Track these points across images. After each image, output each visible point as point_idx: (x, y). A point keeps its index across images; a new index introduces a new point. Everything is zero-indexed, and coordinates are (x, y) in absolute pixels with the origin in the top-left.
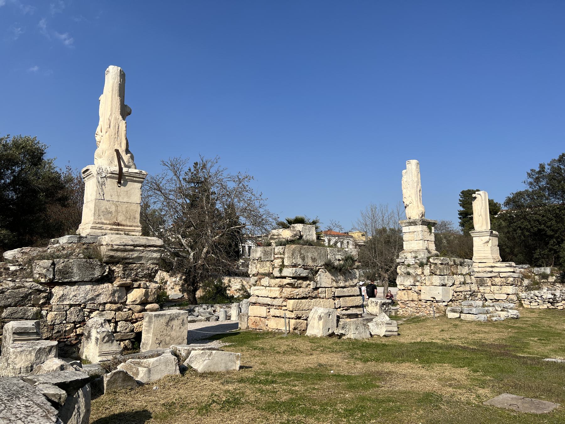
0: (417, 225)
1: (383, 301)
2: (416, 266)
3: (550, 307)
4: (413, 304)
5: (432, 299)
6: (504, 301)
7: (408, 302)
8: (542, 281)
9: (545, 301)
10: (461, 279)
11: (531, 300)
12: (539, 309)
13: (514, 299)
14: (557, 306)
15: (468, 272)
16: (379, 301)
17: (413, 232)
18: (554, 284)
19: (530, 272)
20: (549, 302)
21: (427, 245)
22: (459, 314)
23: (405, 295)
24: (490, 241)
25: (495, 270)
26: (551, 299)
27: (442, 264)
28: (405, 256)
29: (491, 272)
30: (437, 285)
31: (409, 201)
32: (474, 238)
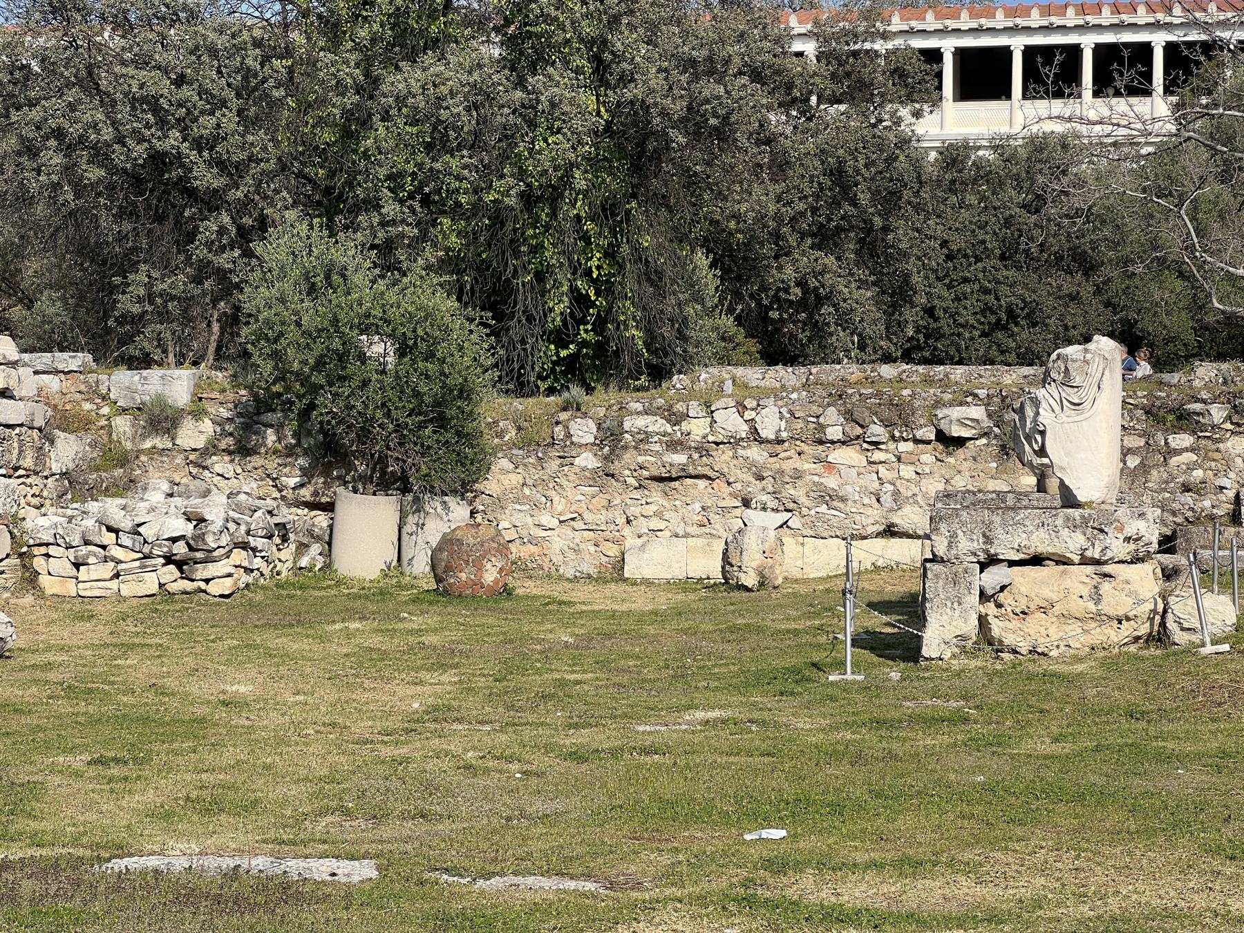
3: (173, 587)
8: (148, 444)
11: (84, 550)
14: (207, 581)
18: (200, 459)
19: (94, 393)
20: (169, 559)
26: (182, 543)
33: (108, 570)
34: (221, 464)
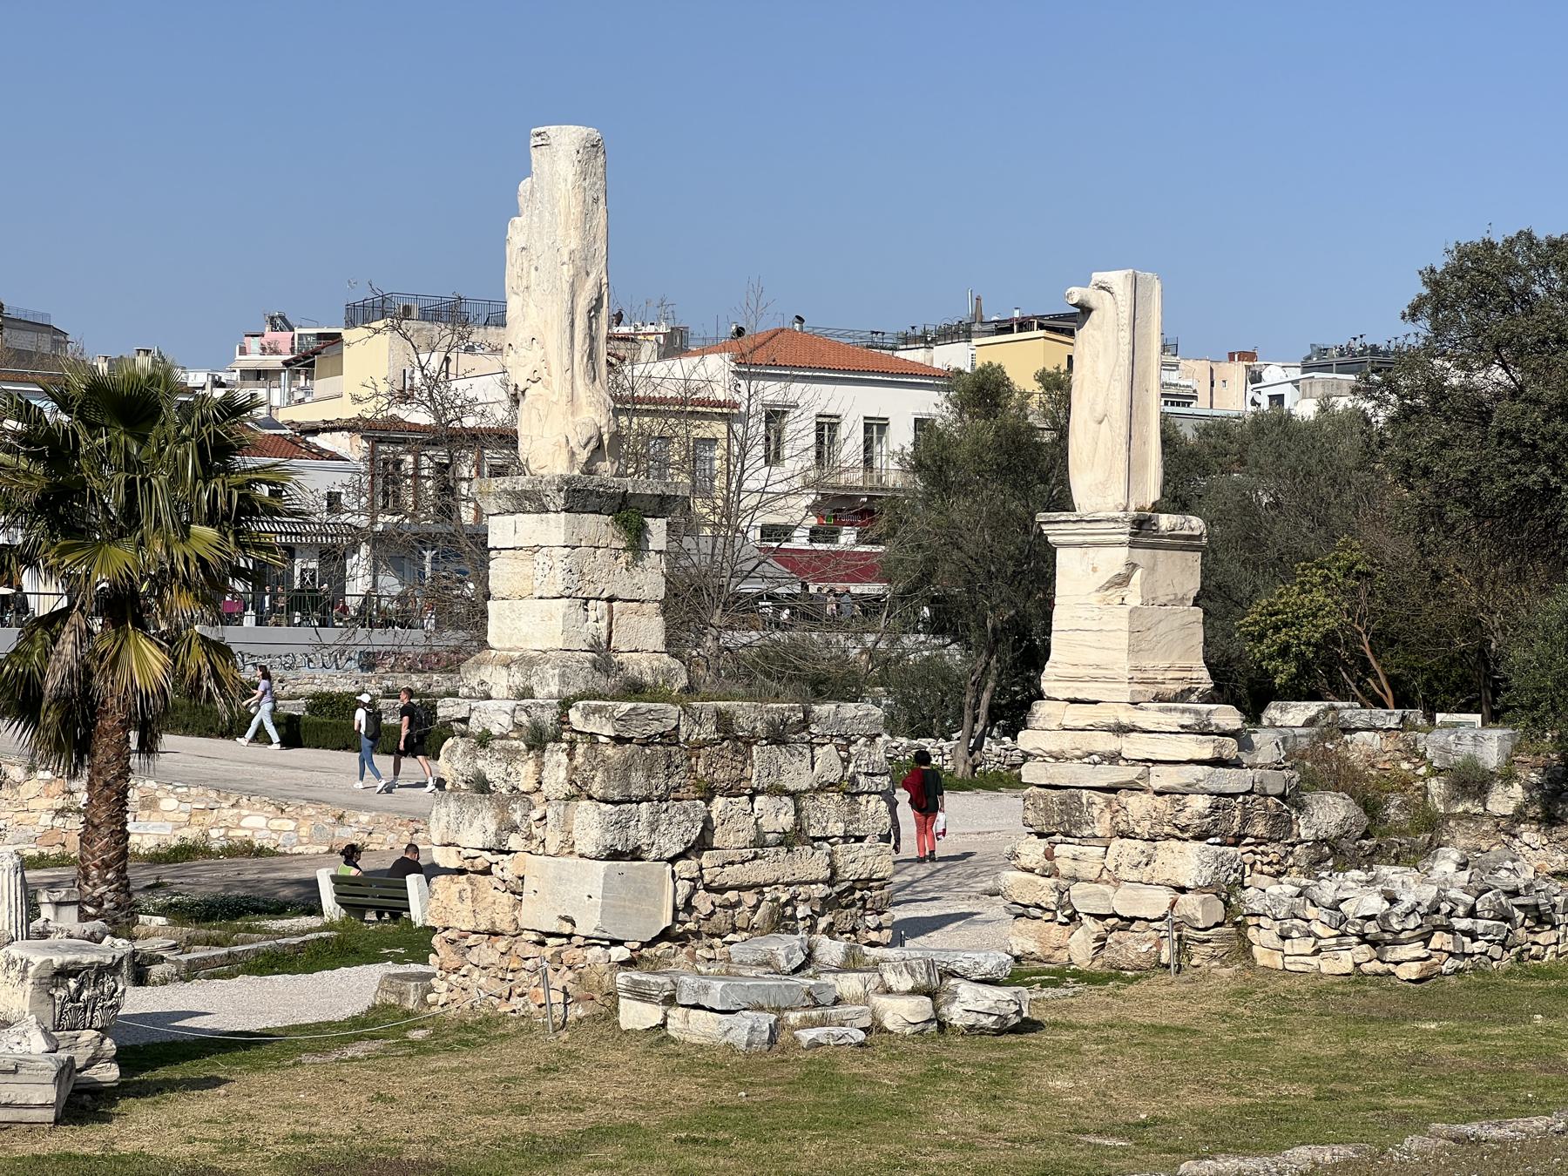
0: (548, 511)
1: (58, 960)
2: (516, 743)
3: (1367, 968)
4: (487, 953)
5: (567, 929)
6: (1156, 925)
7: (472, 939)
8: (1460, 809)
9: (1344, 934)
10: (776, 816)
12: (1320, 975)
13: (1199, 915)
14: (1397, 963)
15: (832, 777)
16: (37, 960)
17: (529, 548)
19: (1412, 752)
20: (1363, 938)
21: (603, 624)
22: (661, 1008)
23: (461, 899)
24: (1137, 577)
25: (1134, 746)
26: (1373, 923)
27: (619, 740)
28: (482, 683)
29: (1114, 758)
30: (588, 854)
31: (530, 368)
32: (1062, 556)
33: (1307, 946)
34: (1529, 835)
